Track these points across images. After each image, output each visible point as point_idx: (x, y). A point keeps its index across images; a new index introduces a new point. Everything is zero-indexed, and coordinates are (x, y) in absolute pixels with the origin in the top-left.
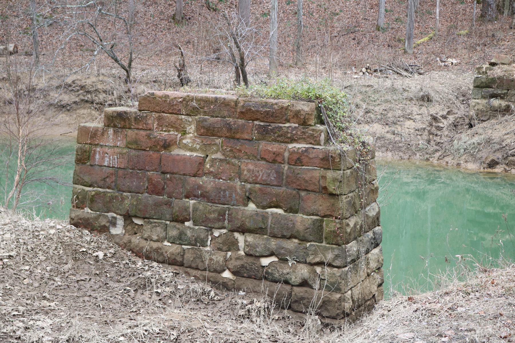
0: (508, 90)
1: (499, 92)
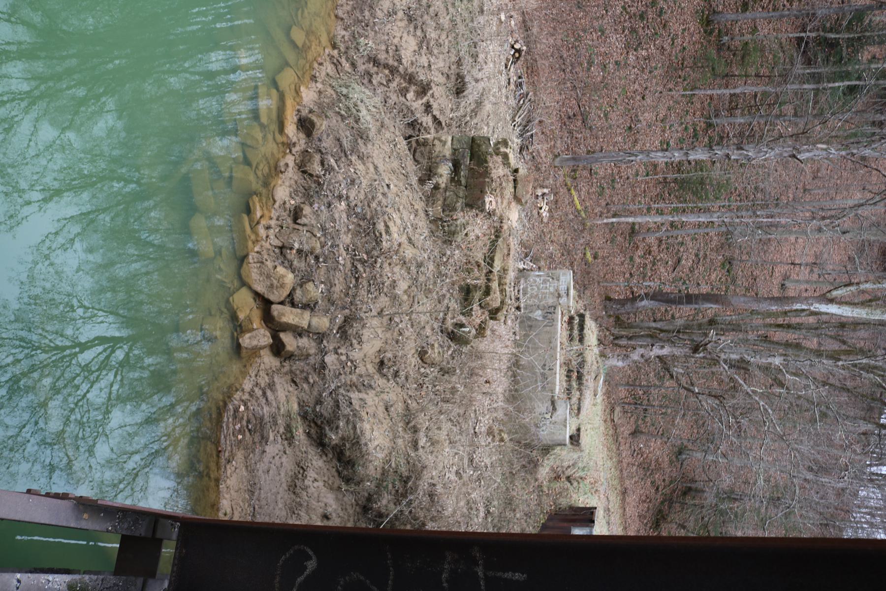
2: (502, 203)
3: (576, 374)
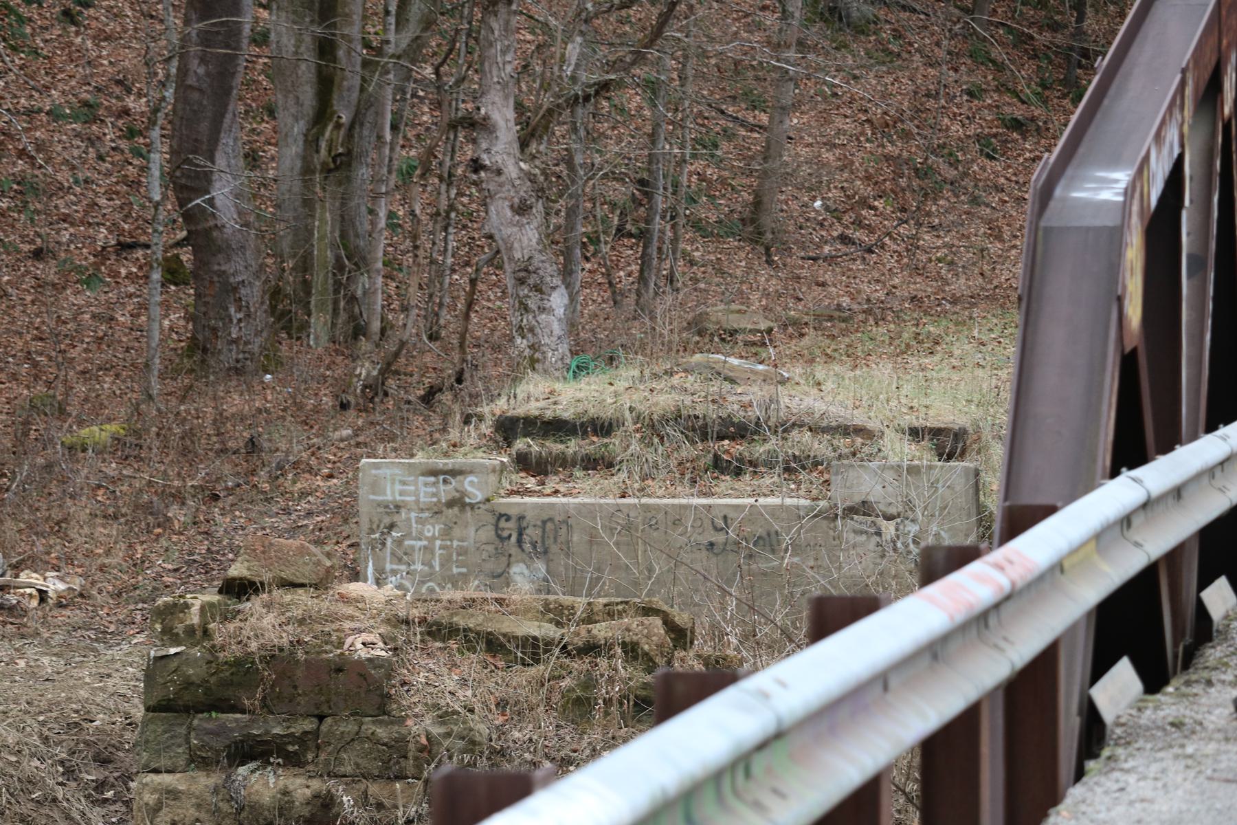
0: (321, 718)
1: (277, 730)
2: (352, 618)
3: (723, 445)
